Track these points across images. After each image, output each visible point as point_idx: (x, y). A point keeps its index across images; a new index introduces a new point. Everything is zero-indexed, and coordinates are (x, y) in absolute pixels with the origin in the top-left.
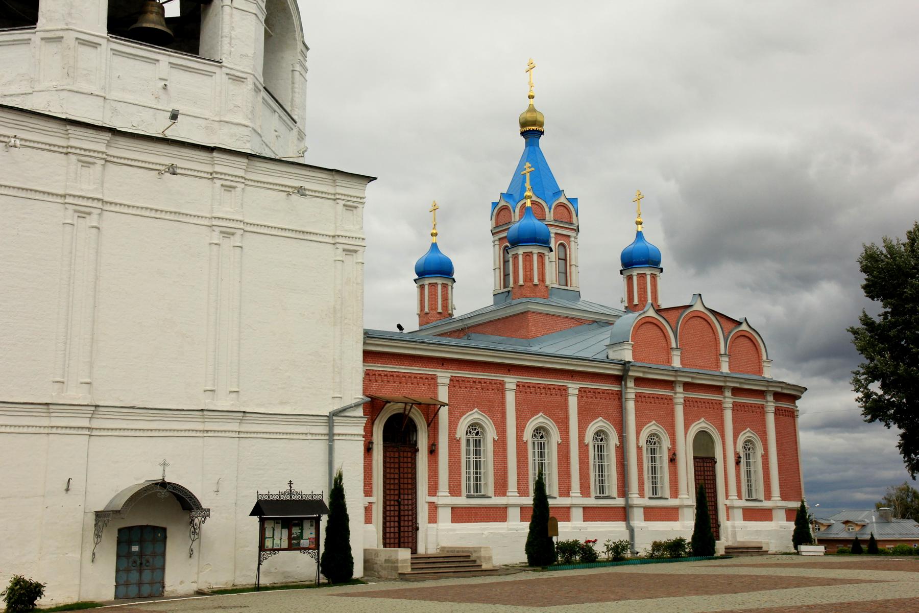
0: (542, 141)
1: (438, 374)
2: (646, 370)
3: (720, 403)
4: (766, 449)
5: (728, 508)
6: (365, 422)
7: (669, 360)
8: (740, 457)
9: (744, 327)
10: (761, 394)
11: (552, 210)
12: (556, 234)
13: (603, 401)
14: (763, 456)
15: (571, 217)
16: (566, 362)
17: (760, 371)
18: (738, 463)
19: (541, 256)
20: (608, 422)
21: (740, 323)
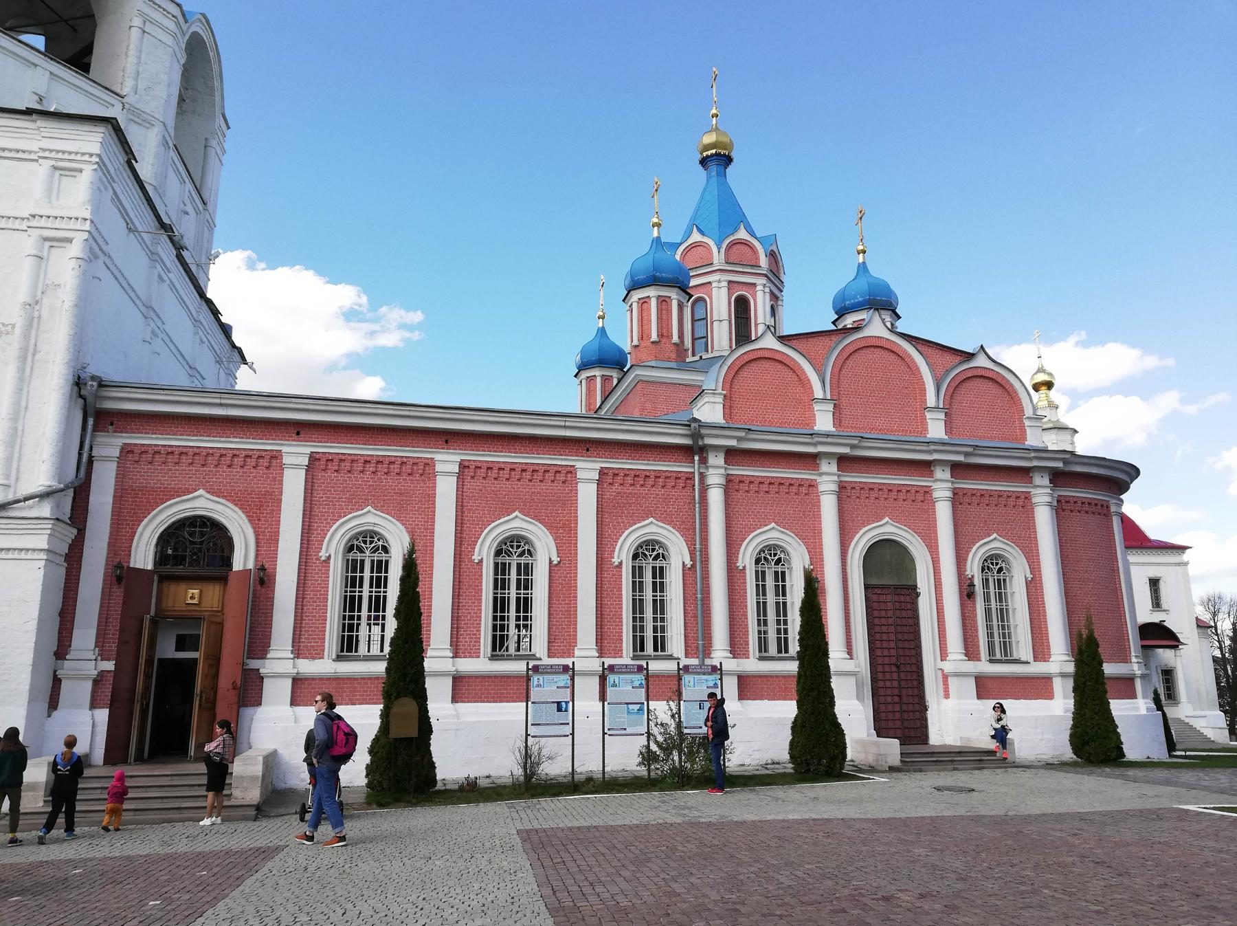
0: (730, 170)
1: (284, 449)
2: (742, 434)
3: (927, 492)
5: (945, 678)
6: (50, 526)
7: (811, 420)
9: (981, 361)
10: (1024, 473)
11: (723, 250)
12: (730, 282)
14: (1029, 584)
15: (757, 258)
18: (967, 593)
19: (663, 302)
21: (970, 356)
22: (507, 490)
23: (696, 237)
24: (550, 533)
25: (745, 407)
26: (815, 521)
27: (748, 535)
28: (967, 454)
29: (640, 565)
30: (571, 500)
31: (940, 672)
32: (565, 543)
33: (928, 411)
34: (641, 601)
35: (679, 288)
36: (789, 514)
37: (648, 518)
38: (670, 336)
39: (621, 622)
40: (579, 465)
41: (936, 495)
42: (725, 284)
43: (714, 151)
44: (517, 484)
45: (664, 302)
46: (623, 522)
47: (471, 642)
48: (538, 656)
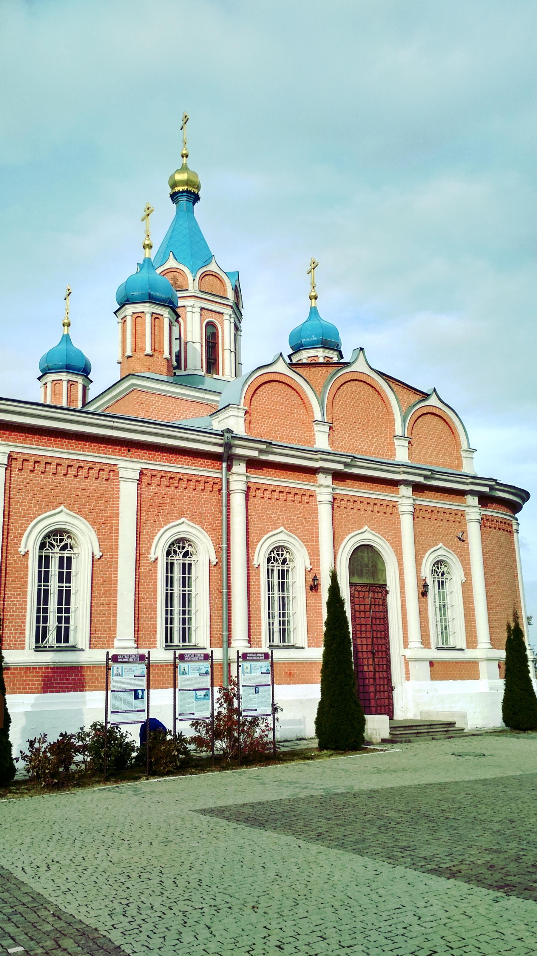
2: (264, 447)
4: (468, 573)
5: (407, 662)
7: (311, 439)
8: (426, 586)
11: (197, 279)
13: (190, 493)
15: (225, 291)
16: (111, 424)
17: (460, 465)
20: (197, 526)
21: (426, 396)
22: (53, 484)
23: (172, 263)
24: (94, 528)
25: (261, 423)
26: (313, 526)
27: (263, 537)
28: (426, 477)
29: (172, 561)
30: (113, 498)
31: (403, 658)
32: (106, 539)
33: (397, 439)
34: (171, 594)
35: (171, 308)
36: (294, 519)
37: (180, 517)
38: (161, 352)
39: (156, 614)
40: (121, 464)
41: (401, 509)
42: (198, 310)
43: (185, 188)
44: (63, 479)
45: (157, 320)
46: (159, 521)
47: (16, 633)
48: (79, 646)
